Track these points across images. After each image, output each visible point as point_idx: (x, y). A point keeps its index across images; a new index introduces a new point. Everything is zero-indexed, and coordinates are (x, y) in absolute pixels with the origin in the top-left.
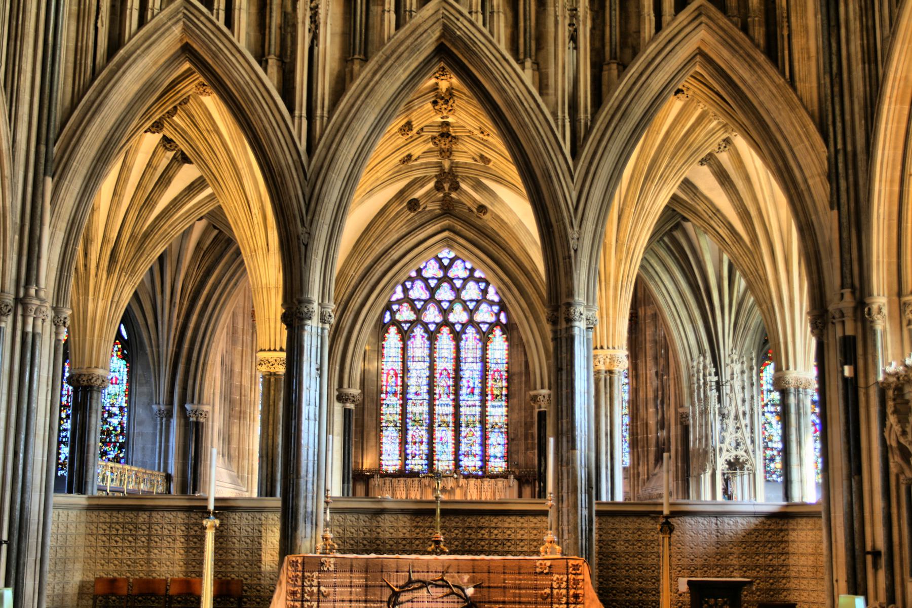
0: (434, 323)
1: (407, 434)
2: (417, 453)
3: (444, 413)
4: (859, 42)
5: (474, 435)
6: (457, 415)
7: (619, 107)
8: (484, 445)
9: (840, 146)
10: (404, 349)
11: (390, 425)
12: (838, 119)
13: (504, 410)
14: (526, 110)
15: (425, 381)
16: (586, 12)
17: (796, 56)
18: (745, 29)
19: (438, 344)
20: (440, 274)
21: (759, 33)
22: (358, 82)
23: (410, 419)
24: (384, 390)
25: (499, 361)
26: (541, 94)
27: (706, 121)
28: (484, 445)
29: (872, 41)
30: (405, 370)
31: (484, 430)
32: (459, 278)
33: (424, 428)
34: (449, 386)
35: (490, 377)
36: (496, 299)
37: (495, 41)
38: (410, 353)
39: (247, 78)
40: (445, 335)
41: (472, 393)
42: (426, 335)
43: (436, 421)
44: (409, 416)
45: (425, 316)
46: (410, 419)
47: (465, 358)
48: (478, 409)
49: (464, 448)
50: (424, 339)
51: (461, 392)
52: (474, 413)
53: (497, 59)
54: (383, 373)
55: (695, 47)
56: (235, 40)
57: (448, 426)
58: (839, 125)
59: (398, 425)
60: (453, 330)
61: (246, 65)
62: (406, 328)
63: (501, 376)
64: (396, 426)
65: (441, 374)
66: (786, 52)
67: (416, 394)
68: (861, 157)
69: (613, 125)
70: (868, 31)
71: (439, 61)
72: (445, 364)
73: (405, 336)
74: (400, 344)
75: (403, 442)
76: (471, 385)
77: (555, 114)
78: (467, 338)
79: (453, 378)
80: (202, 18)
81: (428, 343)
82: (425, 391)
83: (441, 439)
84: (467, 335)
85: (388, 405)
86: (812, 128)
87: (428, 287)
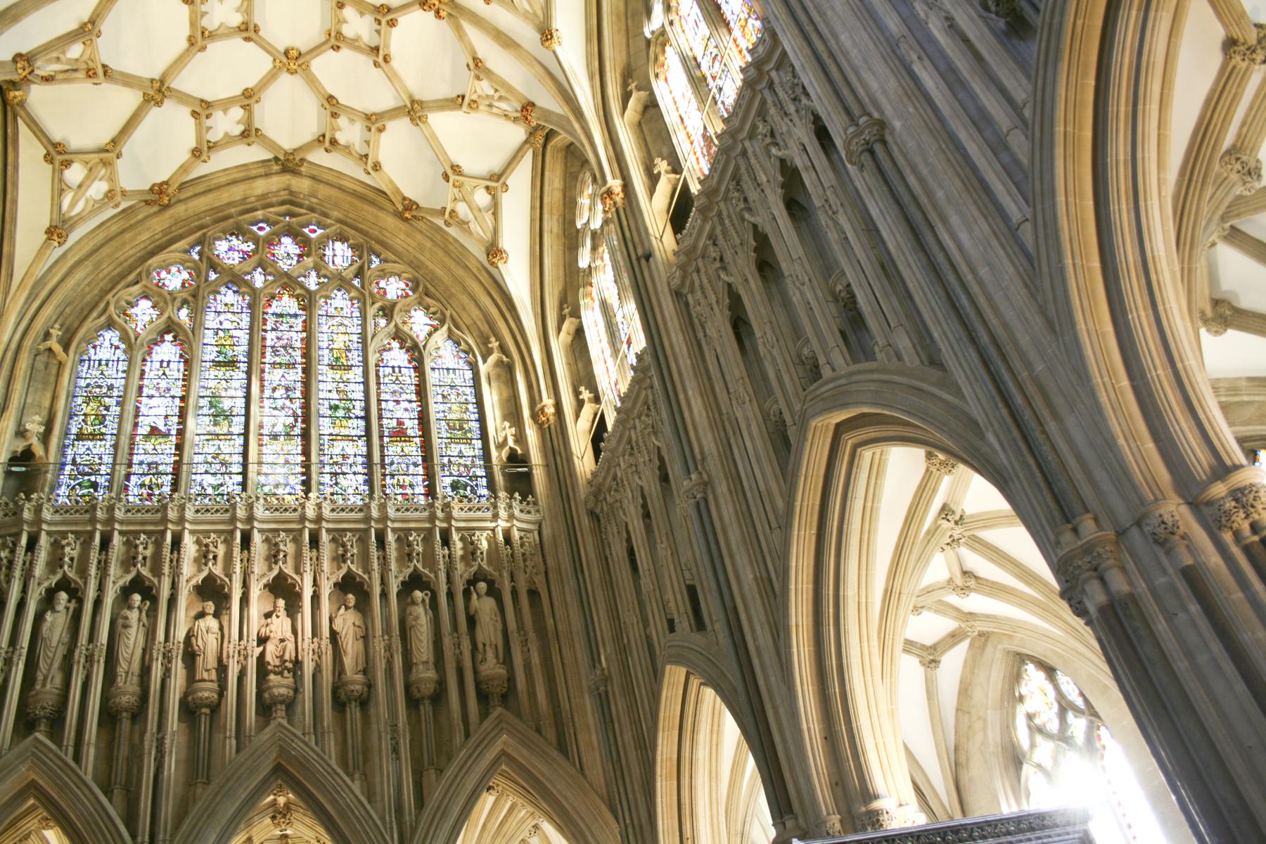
4: (630, 733)
7: (439, 808)
9: (628, 821)
12: (623, 798)
14: (356, 817)
16: (404, 726)
17: (582, 749)
18: (538, 731)
21: (550, 733)
22: (200, 804)
26: (369, 802)
27: (516, 811)
29: (640, 732)
37: (326, 757)
39: (92, 809)
53: (328, 773)
55: (499, 749)
56: (82, 774)
58: (625, 803)
61: (91, 797)
66: (575, 747)
68: (646, 828)
69: (435, 824)
70: (636, 723)
71: (276, 779)
77: (383, 819)
80: (51, 755)
86: (604, 808)
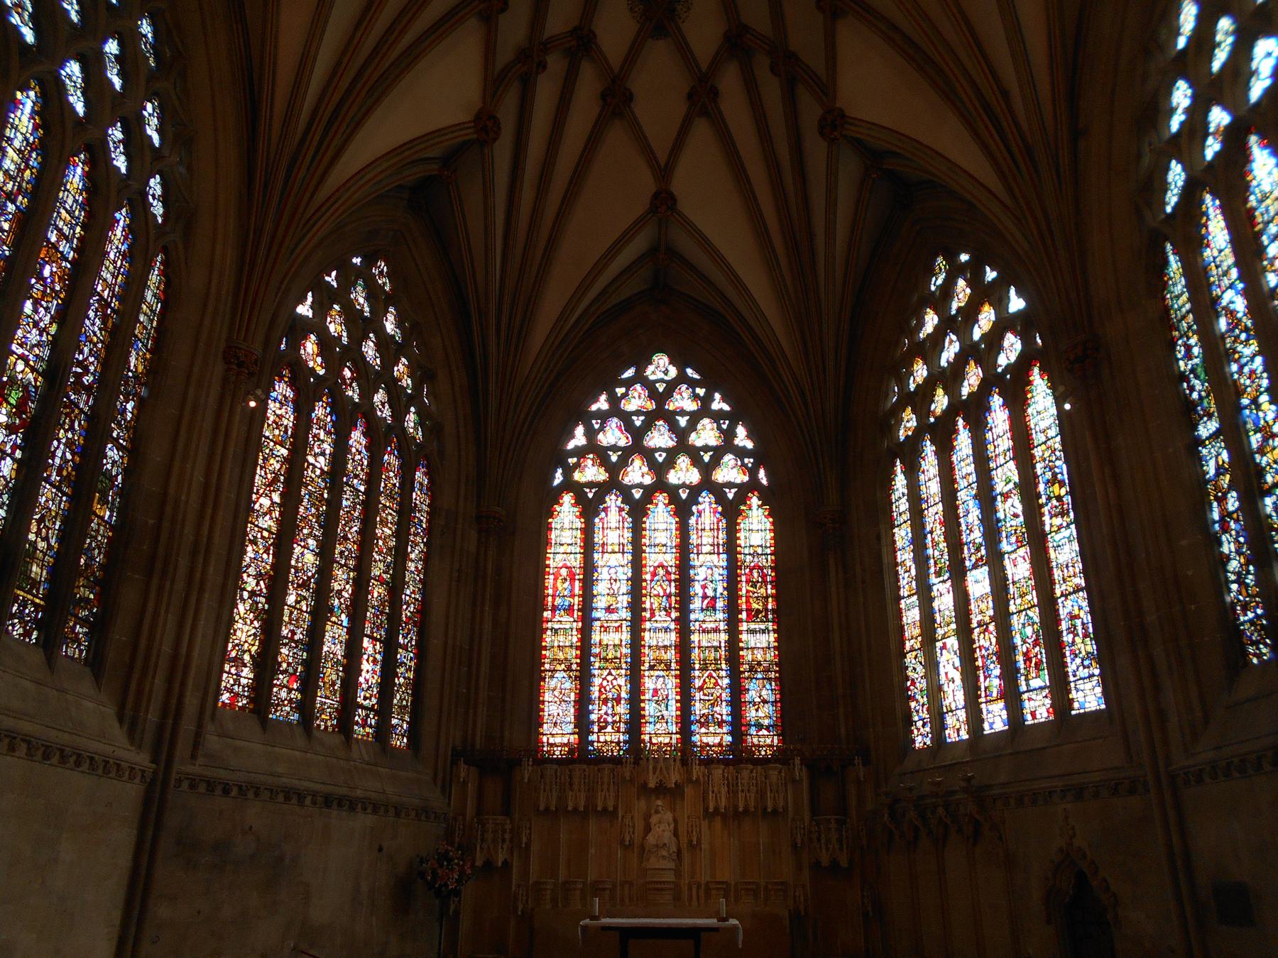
0: (640, 486)
1: (590, 684)
2: (610, 719)
3: (660, 644)
5: (716, 684)
6: (684, 647)
8: (737, 703)
10: (588, 532)
11: (558, 667)
13: (772, 637)
15: (624, 587)
19: (648, 523)
20: (651, 406)
23: (595, 656)
24: (550, 604)
25: (759, 550)
28: (737, 703)
30: (589, 568)
31: (735, 675)
32: (683, 412)
33: (623, 672)
34: (669, 596)
35: (744, 578)
36: (750, 445)
38: (598, 538)
40: (661, 506)
41: (712, 607)
42: (627, 508)
43: (647, 659)
44: (595, 650)
45: (626, 474)
46: (595, 656)
47: (698, 545)
48: (724, 637)
49: (698, 709)
50: (623, 514)
51: (692, 607)
52: (716, 644)
54: (549, 573)
57: (668, 668)
59: (574, 667)
60: (673, 498)
62: (590, 495)
63: (764, 576)
64: (569, 669)
65: (654, 574)
67: (609, 610)
72: (660, 556)
73: (590, 509)
74: (579, 524)
75: (583, 702)
76: (710, 593)
78: (700, 512)
79: (675, 580)
81: (630, 520)
82: (625, 604)
83: (656, 691)
84: (700, 507)
85: (556, 631)
87: (628, 426)
